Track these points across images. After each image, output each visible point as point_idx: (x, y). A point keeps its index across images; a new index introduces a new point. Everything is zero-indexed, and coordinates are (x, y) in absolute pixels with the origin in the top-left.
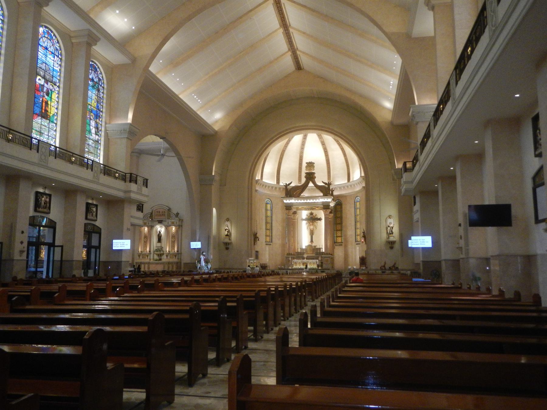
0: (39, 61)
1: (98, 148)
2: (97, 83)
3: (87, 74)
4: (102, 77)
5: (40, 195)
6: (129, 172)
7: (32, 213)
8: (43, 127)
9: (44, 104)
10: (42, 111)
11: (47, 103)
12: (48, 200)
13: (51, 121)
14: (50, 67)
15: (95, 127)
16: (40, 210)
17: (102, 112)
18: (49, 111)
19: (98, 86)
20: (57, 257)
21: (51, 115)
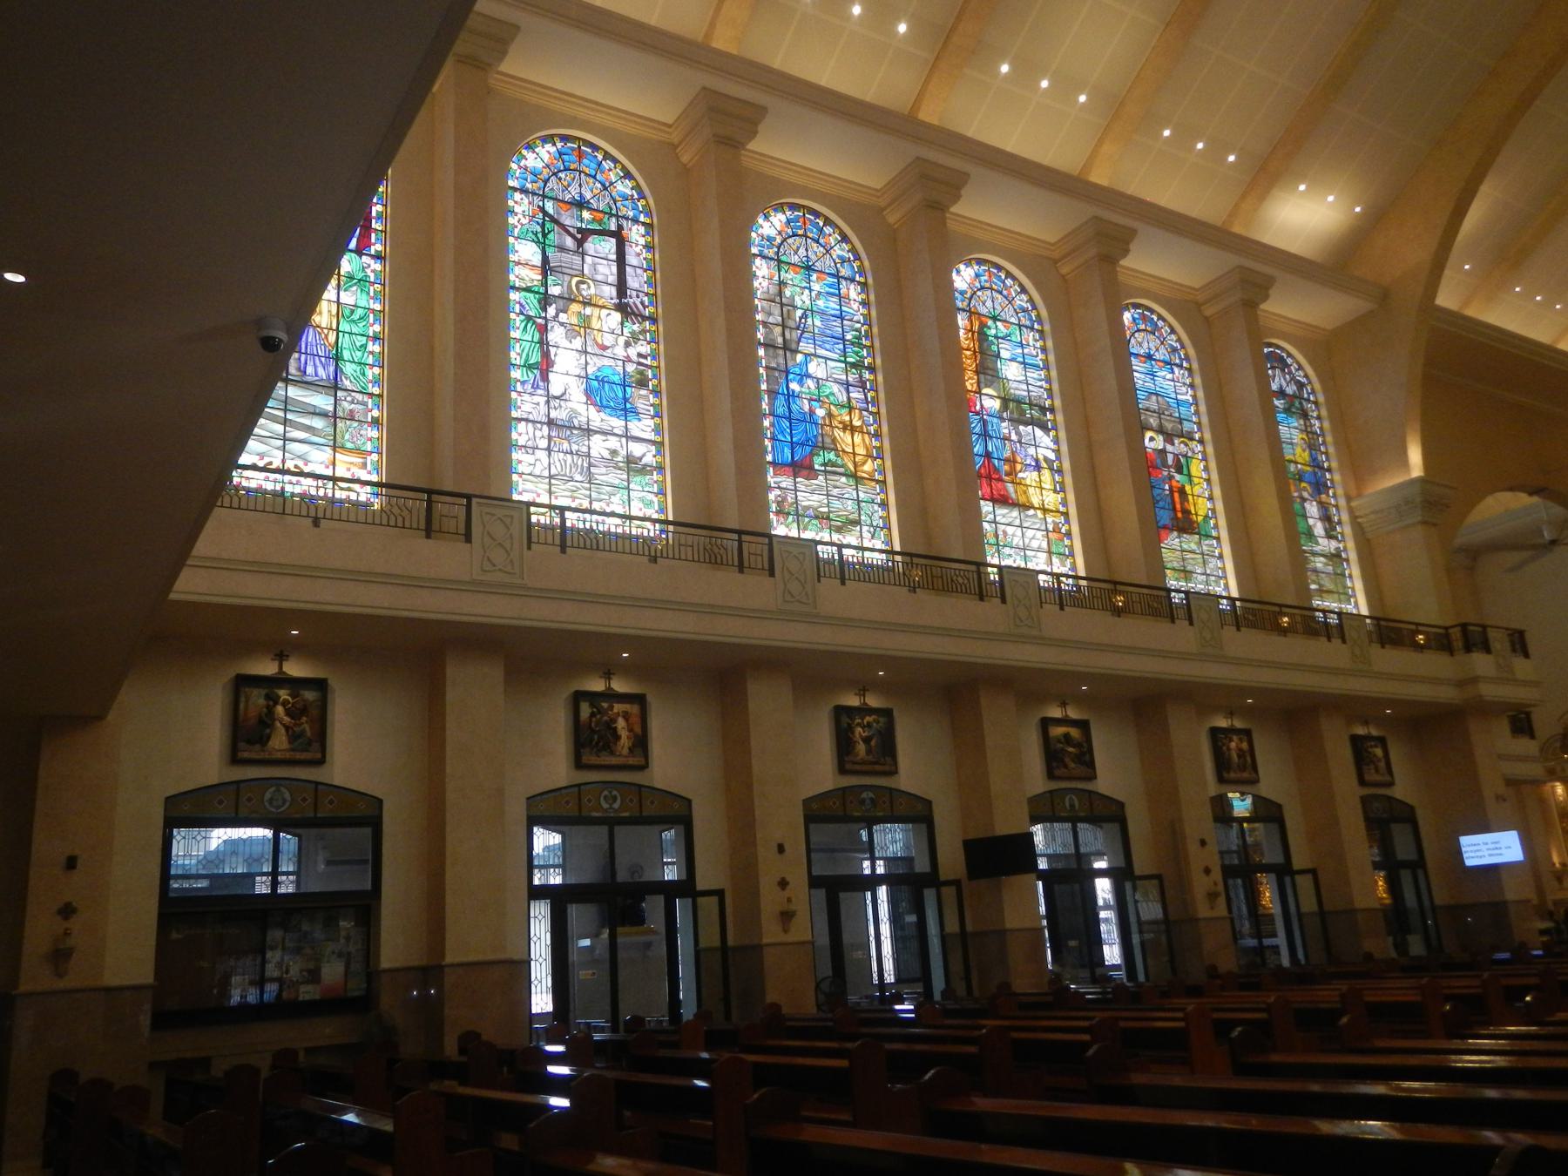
0: (1141, 395)
1: (1344, 575)
2: (1297, 397)
3: (1264, 381)
4: (1306, 376)
5: (1223, 736)
6: (1454, 623)
7: (1213, 789)
8: (1190, 556)
9: (1176, 495)
10: (1176, 515)
11: (1182, 491)
12: (1245, 746)
13: (1204, 535)
14: (1168, 399)
15: (1320, 519)
16: (1232, 775)
17: (1329, 470)
18: (1193, 512)
19: (1301, 403)
20: (1309, 904)
21: (1200, 519)
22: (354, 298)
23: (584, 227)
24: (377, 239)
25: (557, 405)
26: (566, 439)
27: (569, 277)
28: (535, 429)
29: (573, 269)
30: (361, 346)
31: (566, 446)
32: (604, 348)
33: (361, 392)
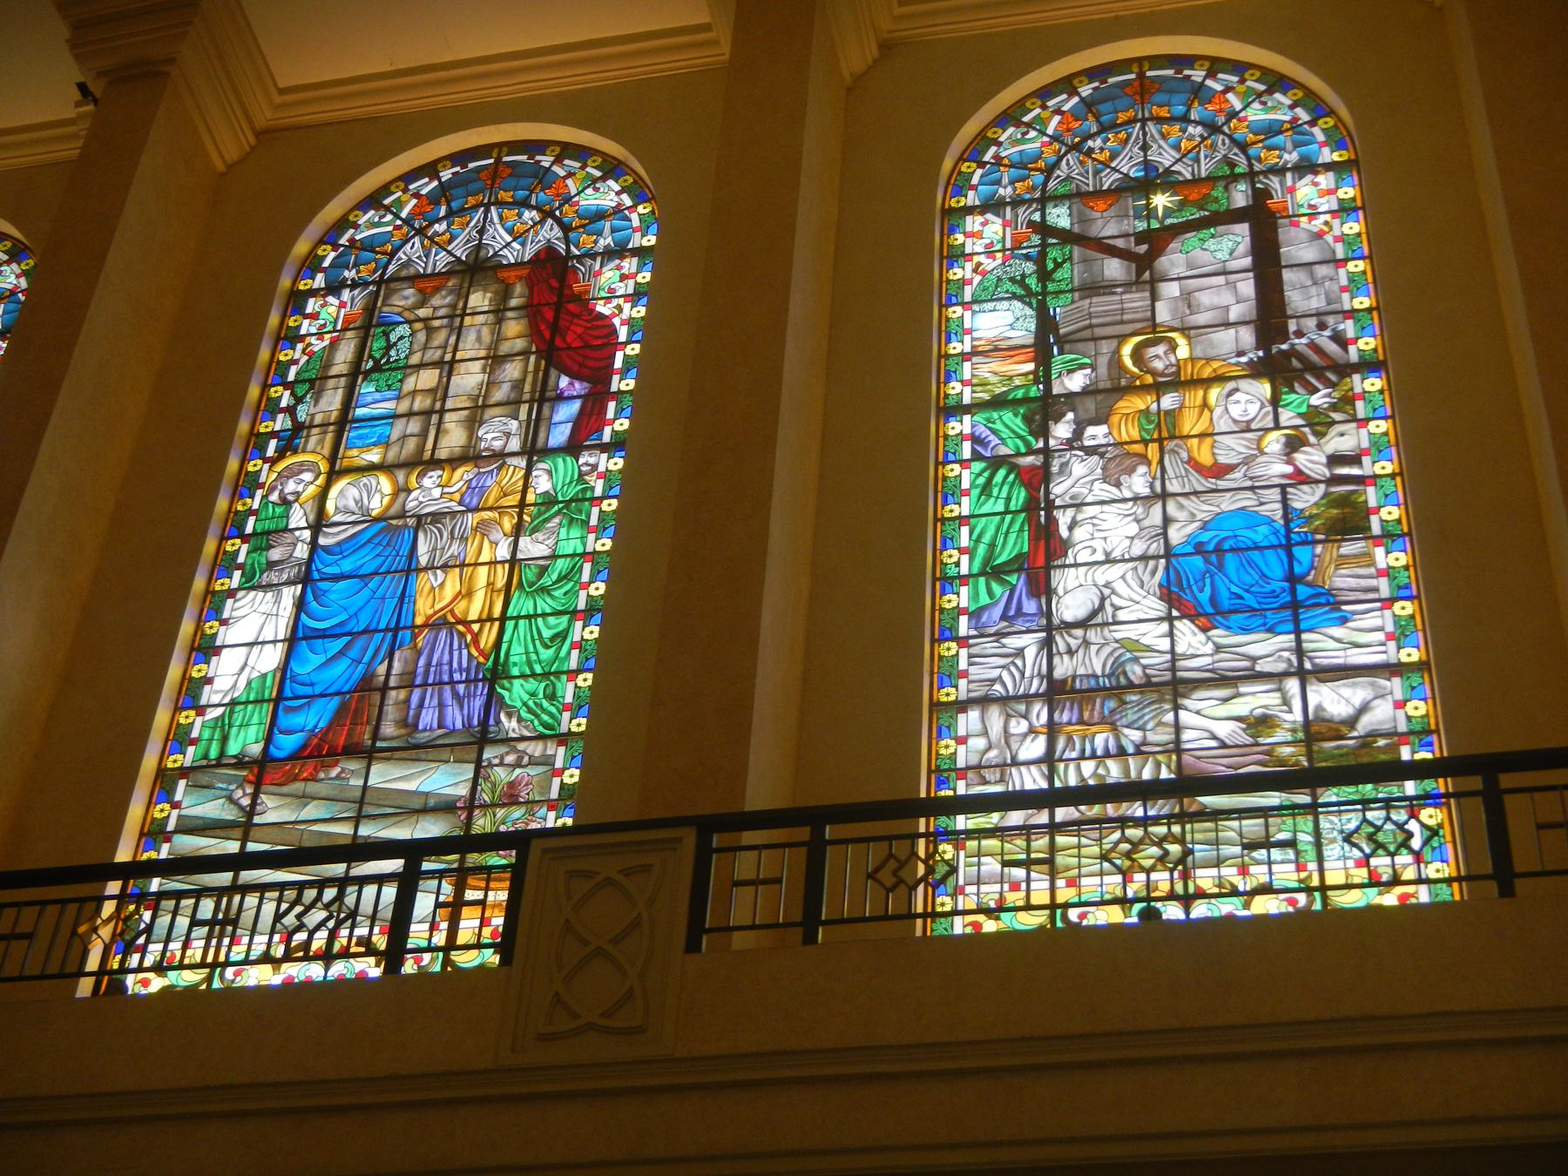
22: (551, 542)
23: (1155, 225)
24: (619, 413)
25: (1074, 643)
26: (1102, 721)
27: (1114, 343)
28: (1008, 716)
29: (1122, 322)
30: (553, 639)
31: (1101, 740)
32: (1220, 471)
33: (541, 737)
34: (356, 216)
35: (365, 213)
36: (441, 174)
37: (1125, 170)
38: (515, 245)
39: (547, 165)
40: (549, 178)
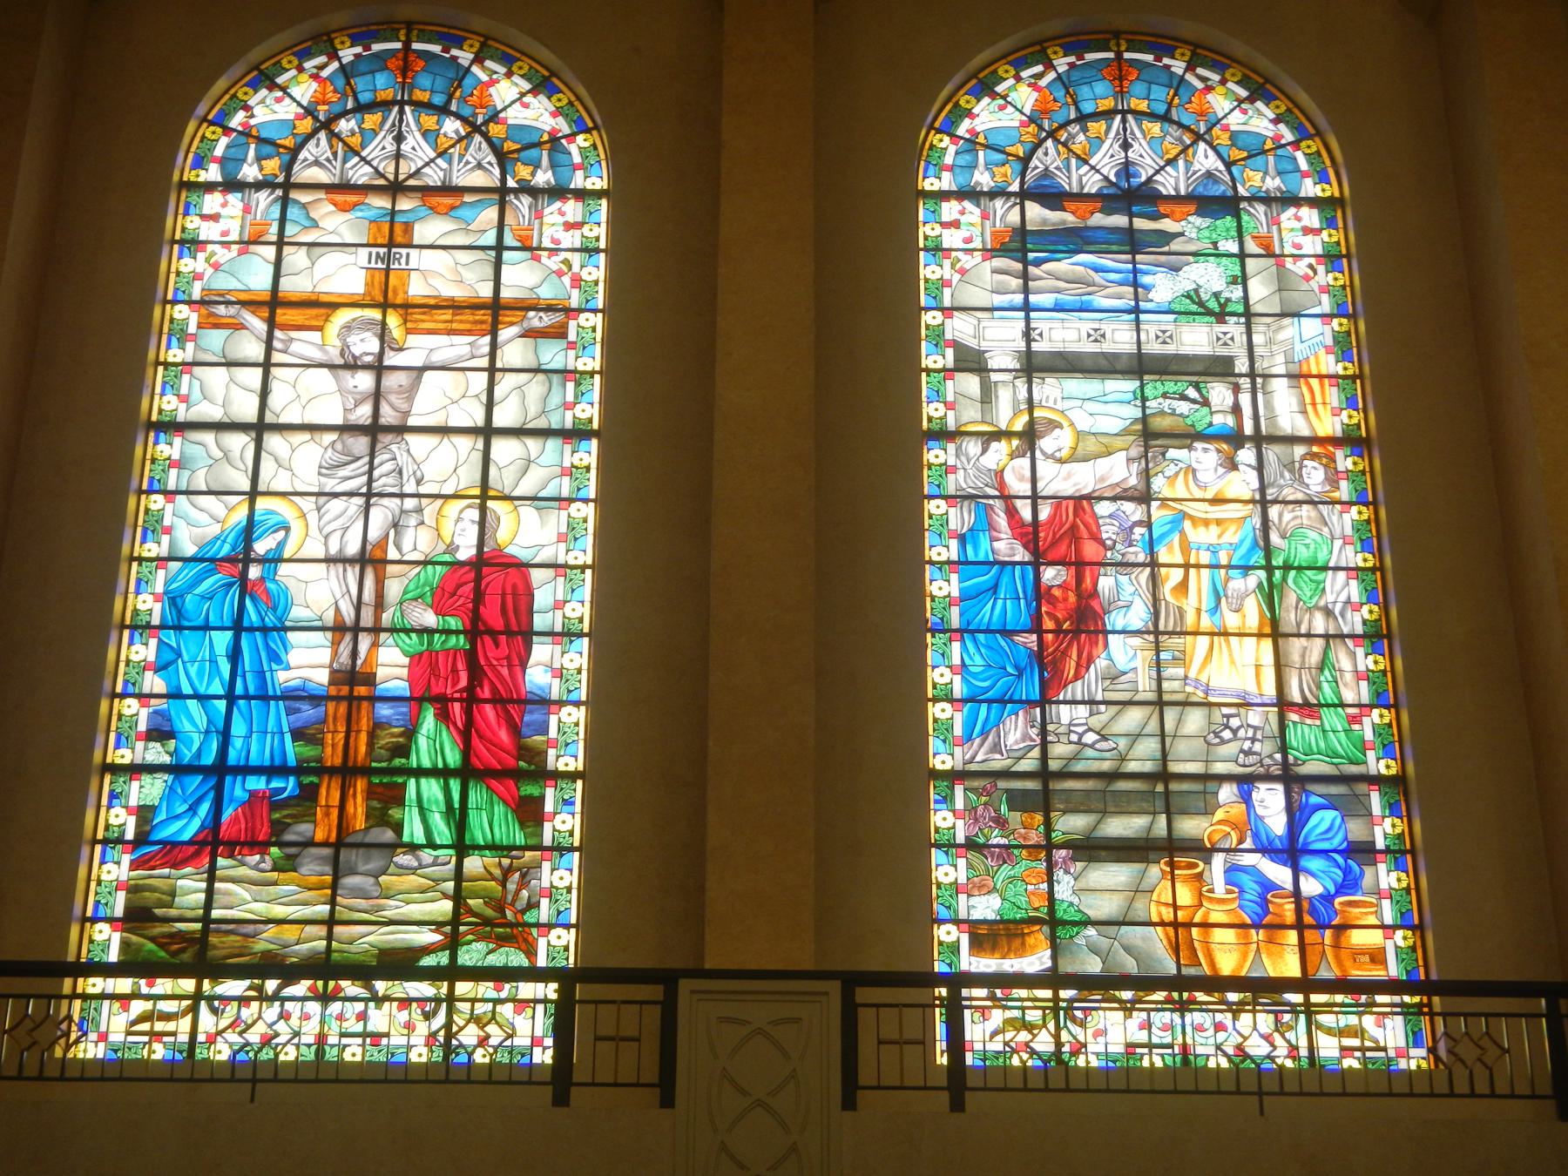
34: (246, 94)
35: (256, 92)
36: (341, 53)
37: (1105, 172)
38: (439, 161)
39: (466, 63)
40: (468, 82)
